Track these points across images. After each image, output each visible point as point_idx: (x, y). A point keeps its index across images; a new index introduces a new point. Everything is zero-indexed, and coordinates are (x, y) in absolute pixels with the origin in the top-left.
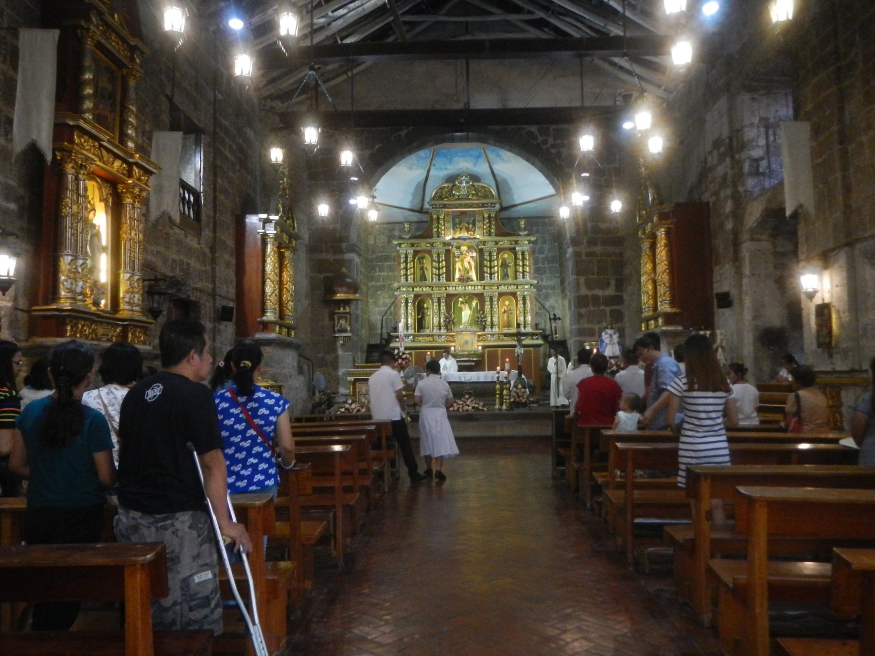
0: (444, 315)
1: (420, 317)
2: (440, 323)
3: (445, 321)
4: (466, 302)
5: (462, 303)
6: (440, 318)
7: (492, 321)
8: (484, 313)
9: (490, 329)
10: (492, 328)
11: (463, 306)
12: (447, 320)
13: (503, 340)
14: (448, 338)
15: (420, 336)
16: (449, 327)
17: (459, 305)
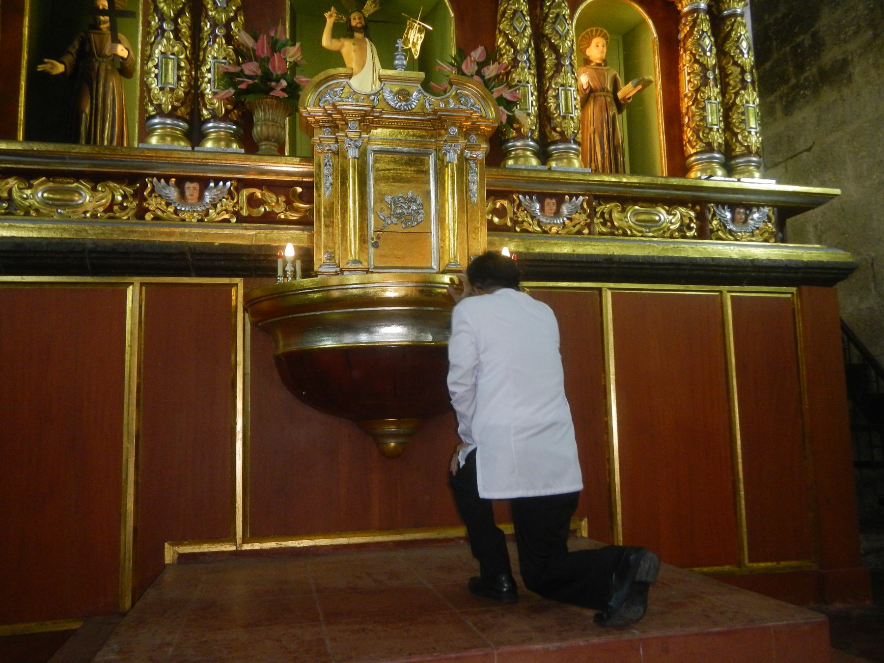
0: (229, 39)
1: (60, 68)
2: (194, 96)
3: (229, 78)
4: (366, 30)
5: (343, 31)
6: (196, 61)
7: (544, 116)
8: (493, 55)
9: (534, 162)
10: (544, 156)
11: (348, 48)
12: (252, 68)
13: (614, 232)
14: (253, 202)
15: (27, 176)
16: (257, 130)
17: (326, 41)
